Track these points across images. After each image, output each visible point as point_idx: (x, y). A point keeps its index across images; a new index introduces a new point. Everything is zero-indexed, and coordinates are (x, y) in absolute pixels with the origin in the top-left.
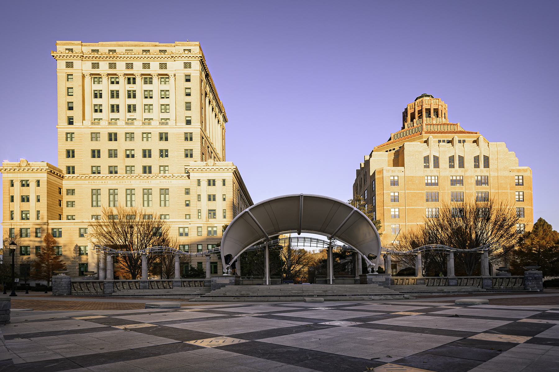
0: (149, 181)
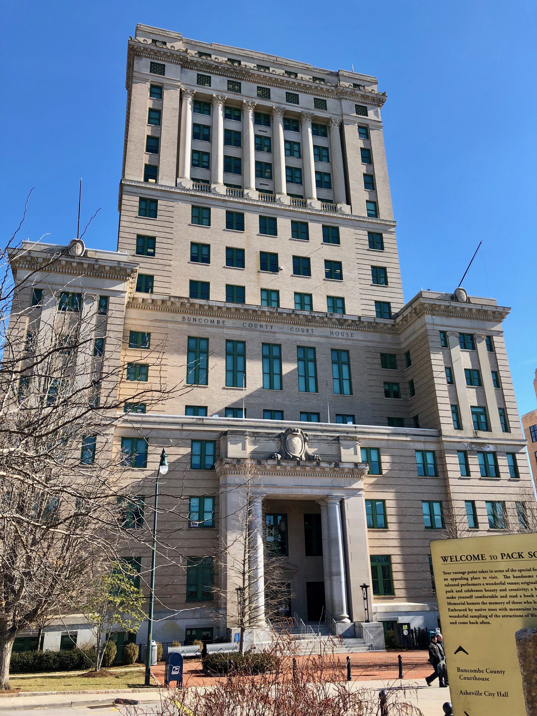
0: (309, 328)
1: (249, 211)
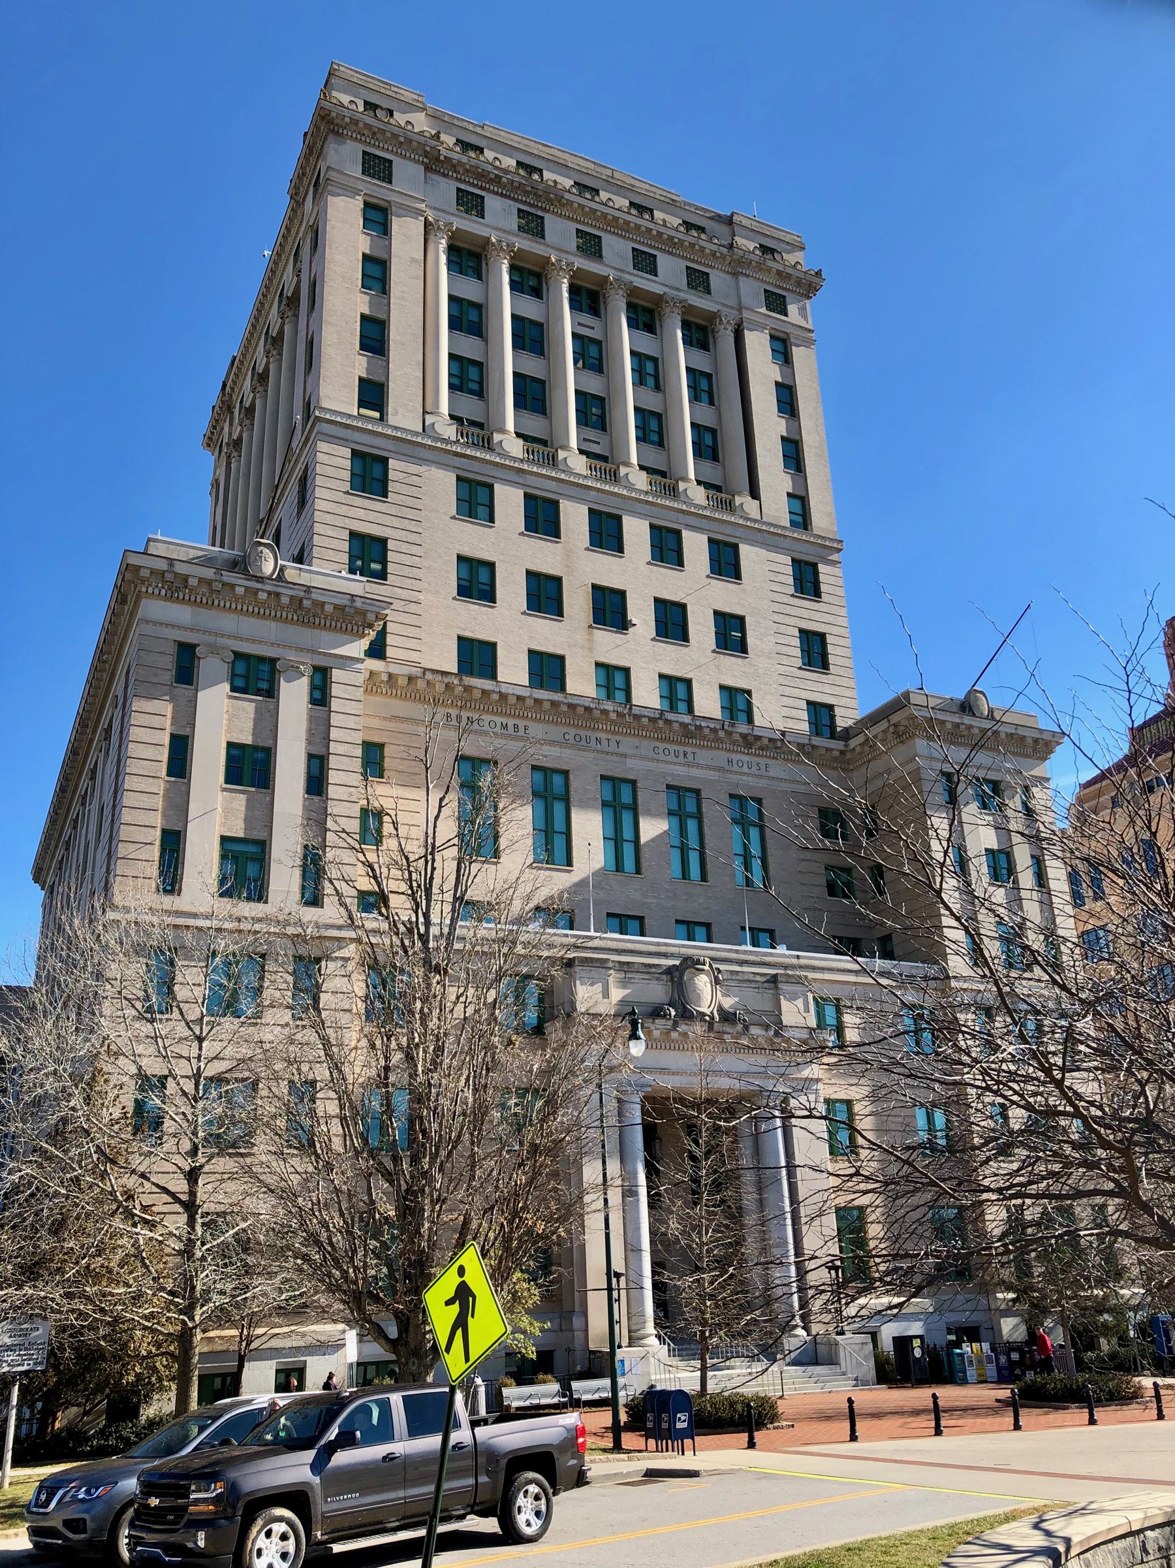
0: (689, 750)
1: (570, 497)
